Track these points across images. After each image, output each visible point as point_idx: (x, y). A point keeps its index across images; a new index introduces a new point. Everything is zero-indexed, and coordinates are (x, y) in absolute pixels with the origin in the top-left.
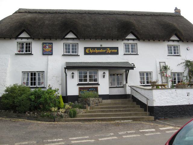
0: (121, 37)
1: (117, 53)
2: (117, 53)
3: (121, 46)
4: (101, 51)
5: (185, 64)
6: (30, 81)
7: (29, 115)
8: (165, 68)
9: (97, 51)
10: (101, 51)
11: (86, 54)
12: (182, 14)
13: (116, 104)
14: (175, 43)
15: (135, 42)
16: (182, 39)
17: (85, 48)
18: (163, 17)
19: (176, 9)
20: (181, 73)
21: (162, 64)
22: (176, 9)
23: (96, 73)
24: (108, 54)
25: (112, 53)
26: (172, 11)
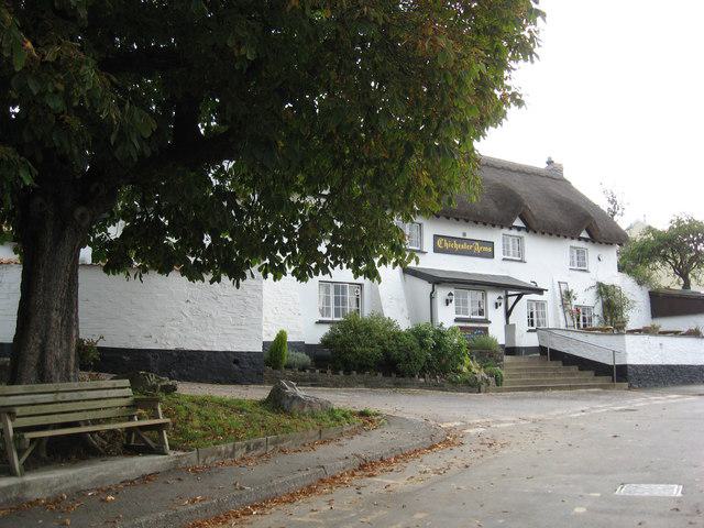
0: (503, 222)
1: (492, 256)
2: (492, 256)
3: (496, 236)
4: (464, 246)
5: (594, 290)
6: (332, 306)
7: (422, 380)
8: (568, 294)
9: (457, 246)
10: (464, 246)
11: (436, 250)
12: (566, 175)
13: (519, 364)
14: (582, 244)
15: (522, 234)
16: (534, 226)
17: (436, 237)
18: (538, 178)
19: (550, 162)
20: (589, 308)
21: (563, 287)
22: (550, 162)
23: (484, 296)
24: (476, 255)
25: (483, 255)
26: (542, 165)
